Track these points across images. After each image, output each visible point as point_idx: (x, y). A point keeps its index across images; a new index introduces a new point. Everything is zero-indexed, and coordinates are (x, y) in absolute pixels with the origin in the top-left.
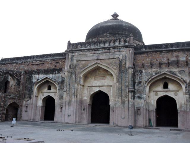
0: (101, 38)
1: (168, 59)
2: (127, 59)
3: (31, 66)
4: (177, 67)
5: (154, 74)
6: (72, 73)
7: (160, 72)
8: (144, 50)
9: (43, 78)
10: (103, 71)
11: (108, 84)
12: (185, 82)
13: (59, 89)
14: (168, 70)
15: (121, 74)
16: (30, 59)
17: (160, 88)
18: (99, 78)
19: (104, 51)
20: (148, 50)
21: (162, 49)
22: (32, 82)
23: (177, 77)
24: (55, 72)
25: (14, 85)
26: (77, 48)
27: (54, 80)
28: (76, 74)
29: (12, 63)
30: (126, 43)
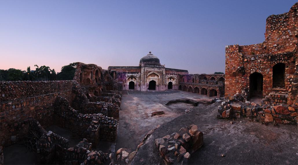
17: (169, 80)
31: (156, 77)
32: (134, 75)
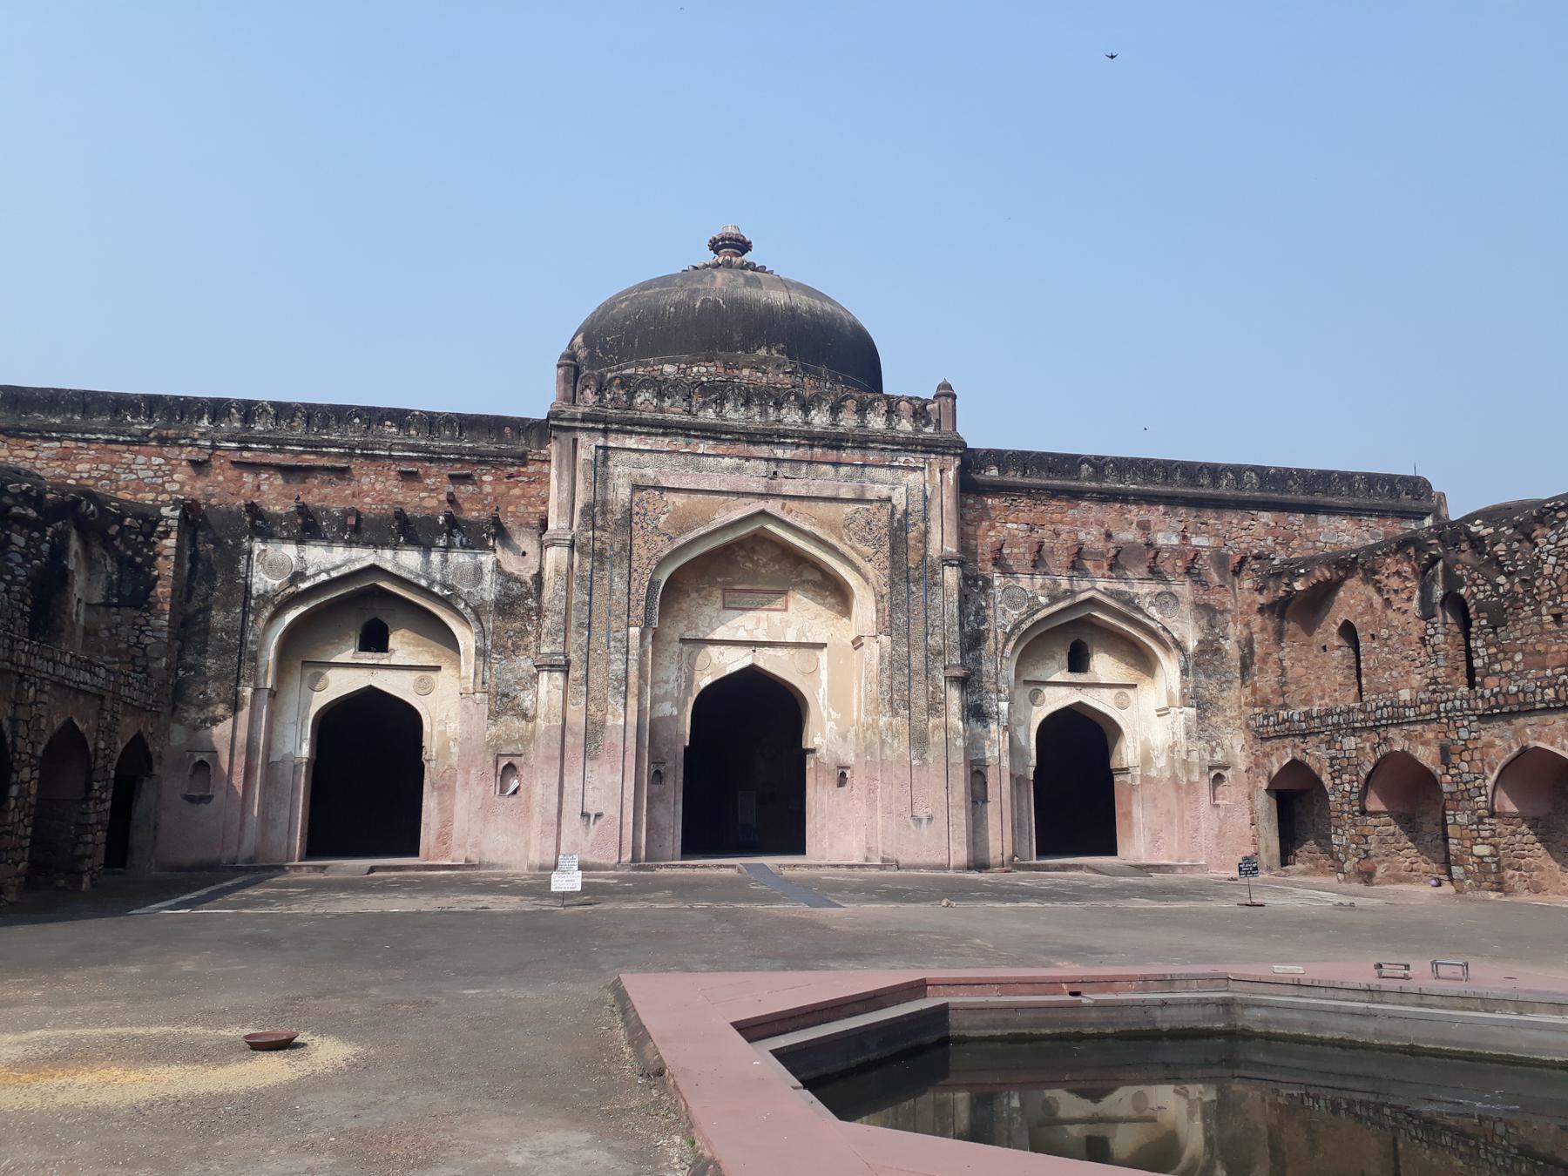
0: (746, 372)
1: (1109, 536)
2: (934, 512)
3: (232, 473)
4: (1145, 575)
5: (1043, 600)
6: (599, 557)
7: (1073, 593)
8: (994, 472)
9: (344, 570)
10: (775, 560)
11: (801, 632)
12: (1180, 646)
13: (481, 653)
14: (1107, 585)
15: (903, 588)
16: (213, 420)
18: (748, 598)
19: (801, 453)
20: (1013, 477)
21: (1078, 479)
22: (247, 588)
23: (1146, 621)
24: (450, 534)
25: (88, 605)
26: (630, 407)
27: (436, 589)
28: (635, 565)
29: (42, 433)
30: (926, 425)
31: (800, 616)
32: (385, 558)
